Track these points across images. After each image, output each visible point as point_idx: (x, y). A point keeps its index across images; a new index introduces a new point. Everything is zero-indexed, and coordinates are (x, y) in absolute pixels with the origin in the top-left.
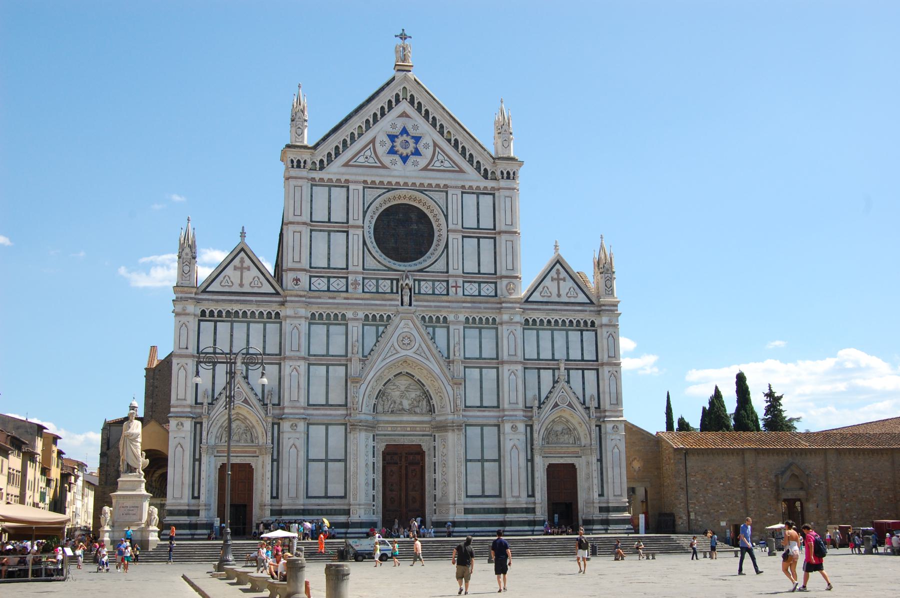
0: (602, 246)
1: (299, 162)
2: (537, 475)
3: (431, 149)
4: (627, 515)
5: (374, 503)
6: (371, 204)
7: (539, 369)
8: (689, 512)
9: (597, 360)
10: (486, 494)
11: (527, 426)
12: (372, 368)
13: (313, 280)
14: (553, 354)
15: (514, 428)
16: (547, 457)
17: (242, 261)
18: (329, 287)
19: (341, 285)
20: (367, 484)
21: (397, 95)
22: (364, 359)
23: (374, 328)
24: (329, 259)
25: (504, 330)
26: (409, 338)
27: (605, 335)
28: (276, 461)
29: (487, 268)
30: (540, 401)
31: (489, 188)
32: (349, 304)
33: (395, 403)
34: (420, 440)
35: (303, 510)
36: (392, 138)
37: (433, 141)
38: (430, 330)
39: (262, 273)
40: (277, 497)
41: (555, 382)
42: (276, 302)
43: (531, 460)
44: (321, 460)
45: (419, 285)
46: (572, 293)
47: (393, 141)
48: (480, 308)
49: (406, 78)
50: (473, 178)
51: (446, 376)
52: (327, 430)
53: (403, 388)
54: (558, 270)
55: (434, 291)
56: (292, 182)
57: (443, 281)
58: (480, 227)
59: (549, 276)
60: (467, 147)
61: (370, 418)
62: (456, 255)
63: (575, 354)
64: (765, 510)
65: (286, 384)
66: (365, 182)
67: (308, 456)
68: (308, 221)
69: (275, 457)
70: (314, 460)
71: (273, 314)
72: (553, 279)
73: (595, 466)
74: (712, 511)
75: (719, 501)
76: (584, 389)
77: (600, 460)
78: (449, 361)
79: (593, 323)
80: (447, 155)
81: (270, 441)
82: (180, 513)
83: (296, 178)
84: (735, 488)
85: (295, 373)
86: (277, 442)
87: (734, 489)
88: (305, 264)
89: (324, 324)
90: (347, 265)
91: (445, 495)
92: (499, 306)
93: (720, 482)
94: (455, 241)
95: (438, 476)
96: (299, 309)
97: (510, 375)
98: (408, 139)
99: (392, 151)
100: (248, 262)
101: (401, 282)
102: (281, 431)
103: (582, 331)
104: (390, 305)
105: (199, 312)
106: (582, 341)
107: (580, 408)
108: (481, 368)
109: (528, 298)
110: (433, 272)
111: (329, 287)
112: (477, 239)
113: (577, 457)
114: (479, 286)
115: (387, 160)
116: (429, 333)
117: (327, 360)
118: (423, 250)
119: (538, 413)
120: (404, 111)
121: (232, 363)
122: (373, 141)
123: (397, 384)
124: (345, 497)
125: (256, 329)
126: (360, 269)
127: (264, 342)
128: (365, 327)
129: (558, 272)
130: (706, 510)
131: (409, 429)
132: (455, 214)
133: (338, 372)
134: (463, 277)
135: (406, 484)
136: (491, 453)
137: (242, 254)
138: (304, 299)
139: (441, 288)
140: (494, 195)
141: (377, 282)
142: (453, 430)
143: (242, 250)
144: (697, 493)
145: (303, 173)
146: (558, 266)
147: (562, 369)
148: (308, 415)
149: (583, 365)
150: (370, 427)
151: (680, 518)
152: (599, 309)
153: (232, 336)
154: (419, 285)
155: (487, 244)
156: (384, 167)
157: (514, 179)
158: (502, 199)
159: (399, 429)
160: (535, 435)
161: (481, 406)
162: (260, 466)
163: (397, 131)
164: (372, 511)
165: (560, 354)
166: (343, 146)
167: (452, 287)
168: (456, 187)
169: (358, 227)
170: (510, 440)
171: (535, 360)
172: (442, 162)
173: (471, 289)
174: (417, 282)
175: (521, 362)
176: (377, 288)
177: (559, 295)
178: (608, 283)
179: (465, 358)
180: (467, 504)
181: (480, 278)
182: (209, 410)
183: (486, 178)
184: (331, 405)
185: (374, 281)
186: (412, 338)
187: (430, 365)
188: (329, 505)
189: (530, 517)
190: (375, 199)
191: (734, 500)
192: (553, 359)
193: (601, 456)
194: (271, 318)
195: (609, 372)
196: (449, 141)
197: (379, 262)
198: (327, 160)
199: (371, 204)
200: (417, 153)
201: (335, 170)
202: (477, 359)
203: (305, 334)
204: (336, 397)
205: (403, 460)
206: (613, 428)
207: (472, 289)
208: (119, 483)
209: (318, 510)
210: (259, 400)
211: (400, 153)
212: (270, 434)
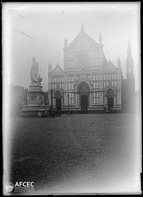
17: (58, 68)
28: (63, 99)
38: (87, 76)
41: (109, 84)
133: (73, 84)
143: (58, 65)
146: (110, 63)
150: (78, 93)
187: (87, 82)
212: (62, 95)
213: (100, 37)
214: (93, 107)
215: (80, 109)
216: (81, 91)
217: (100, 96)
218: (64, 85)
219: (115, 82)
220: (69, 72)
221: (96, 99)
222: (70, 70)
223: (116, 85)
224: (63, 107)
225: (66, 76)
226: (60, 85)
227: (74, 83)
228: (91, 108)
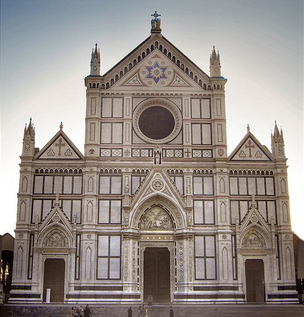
0: (276, 126)
2: (239, 266)
3: (172, 74)
4: (295, 292)
6: (137, 106)
7: (239, 201)
9: (275, 195)
11: (232, 236)
13: (102, 150)
14: (248, 192)
15: (224, 237)
17: (60, 141)
18: (111, 155)
19: (119, 153)
20: (134, 271)
21: (152, 46)
22: (132, 197)
24: (112, 138)
25: (217, 178)
27: (280, 179)
28: (78, 257)
29: (207, 141)
30: (240, 220)
32: (123, 164)
35: (94, 287)
36: (149, 69)
39: (72, 148)
40: (79, 279)
41: (249, 209)
42: (80, 163)
44: (106, 257)
45: (166, 152)
47: (150, 71)
48: (203, 164)
49: (157, 36)
51: (182, 206)
52: (109, 238)
53: (156, 214)
55: (174, 155)
56: (90, 96)
57: (180, 149)
60: (193, 73)
61: (136, 231)
63: (261, 192)
65: (85, 211)
66: (133, 94)
69: (78, 255)
70: (101, 257)
73: (275, 261)
76: (267, 213)
77: (278, 257)
79: (271, 172)
82: (20, 288)
83: (93, 93)
85: (90, 204)
86: (79, 245)
88: (97, 141)
90: (123, 142)
91: (182, 278)
92: (214, 163)
95: (178, 267)
96: (93, 168)
97: (221, 204)
98: (159, 69)
99: (149, 76)
100: (64, 141)
101: (154, 150)
102: (82, 239)
103: (265, 177)
104: (148, 164)
107: (266, 225)
108: (204, 200)
109: (231, 159)
111: (111, 155)
113: (263, 255)
114: (202, 152)
115: (146, 81)
116: (171, 180)
117: (110, 197)
120: (156, 55)
121: (52, 200)
122: (138, 71)
123: (153, 211)
124: (120, 279)
125: (68, 179)
127: (73, 187)
129: (250, 143)
131: (160, 238)
132: (187, 111)
136: (210, 253)
137: (61, 137)
139: (179, 153)
140: (210, 99)
141: (140, 151)
142: (187, 238)
143: (61, 135)
146: (249, 139)
147: (254, 200)
148: (98, 229)
149: (266, 198)
150: (136, 237)
152: (275, 164)
153: (53, 183)
154: (166, 152)
155: (206, 128)
156: (144, 85)
158: (215, 101)
159: (154, 238)
160: (238, 241)
162: (69, 259)
163: (153, 65)
165: (252, 192)
168: (187, 95)
169: (129, 119)
171: (237, 195)
172: (179, 81)
173: (197, 154)
174: (164, 150)
176: (140, 155)
177: (250, 156)
178: (281, 148)
180: (196, 284)
182: (38, 227)
185: (139, 151)
186: (161, 183)
190: (139, 104)
192: (248, 195)
194: (77, 173)
196: (183, 69)
197: (142, 139)
199: (137, 106)
200: (164, 77)
201: (116, 88)
204: (116, 219)
206: (286, 236)
207: (197, 154)
209: (103, 287)
210: (69, 221)
212: (75, 241)
214: (197, 292)
215: (141, 299)
216: (145, 232)
220: (106, 159)
221: (205, 260)
222: (107, 153)
224: (76, 288)
225: (92, 172)
226: (67, 204)
227: (121, 200)
228: (188, 296)
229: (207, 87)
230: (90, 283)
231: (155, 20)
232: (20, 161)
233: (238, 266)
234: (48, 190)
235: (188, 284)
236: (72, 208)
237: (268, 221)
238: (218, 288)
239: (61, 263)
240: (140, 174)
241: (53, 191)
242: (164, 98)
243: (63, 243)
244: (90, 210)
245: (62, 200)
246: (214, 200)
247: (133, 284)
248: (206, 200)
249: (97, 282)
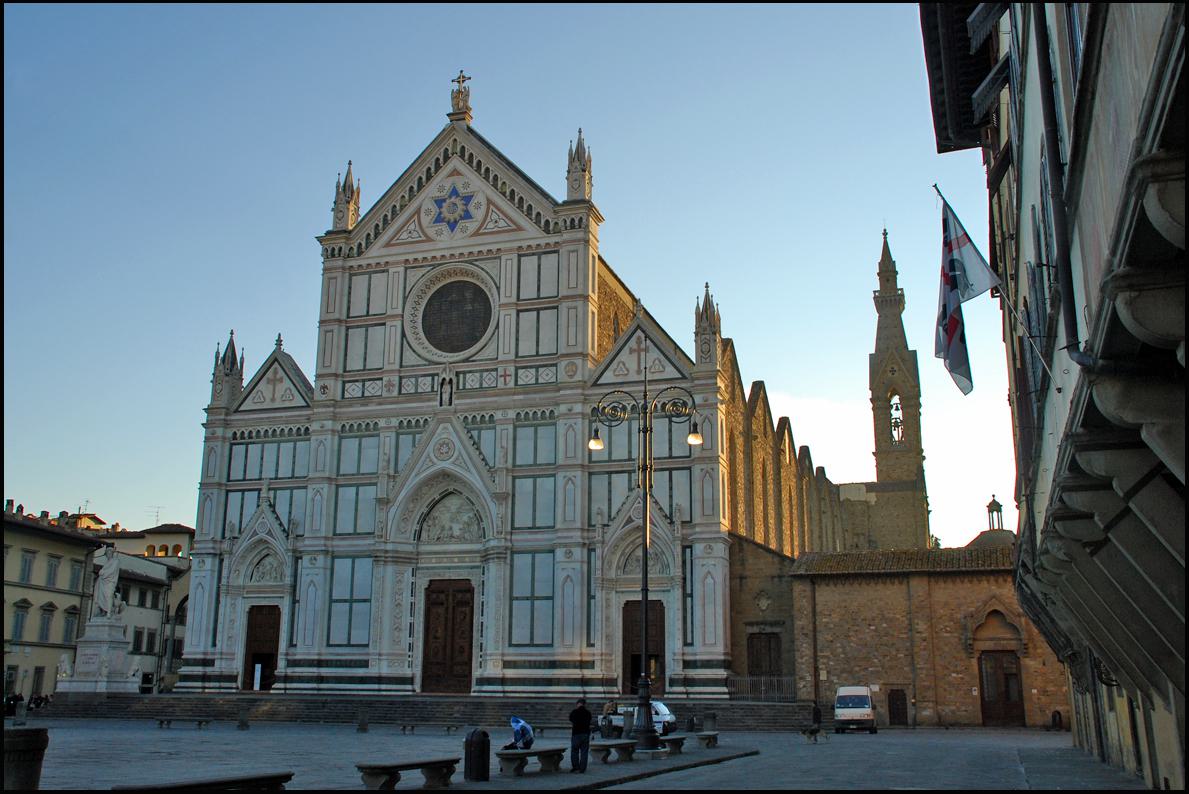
1: (333, 249)
3: (483, 208)
4: (722, 673)
5: (410, 653)
8: (816, 670)
10: (535, 643)
12: (403, 486)
13: (347, 385)
15: (569, 554)
16: (623, 592)
17: (276, 372)
20: (398, 628)
23: (411, 437)
24: (365, 359)
25: (561, 428)
26: (447, 445)
28: (294, 602)
30: (610, 516)
31: (552, 244)
33: (443, 528)
34: (469, 574)
36: (439, 202)
37: (488, 200)
41: (631, 489)
43: (590, 597)
44: (345, 601)
45: (464, 378)
46: (658, 367)
47: (440, 207)
48: (535, 399)
49: (454, 128)
50: (532, 235)
52: (353, 563)
53: (453, 509)
54: (639, 338)
55: (481, 384)
57: (493, 370)
58: (541, 296)
59: (626, 348)
61: (410, 548)
62: (507, 335)
64: (948, 668)
67: (331, 596)
68: (344, 317)
69: (297, 598)
71: (303, 430)
72: (631, 351)
74: (857, 669)
75: (869, 653)
76: (671, 497)
78: (492, 471)
80: (502, 212)
81: (288, 580)
84: (895, 634)
87: (893, 635)
89: (356, 437)
92: (557, 394)
93: (870, 625)
94: (503, 317)
95: (484, 619)
96: (325, 422)
97: (567, 483)
99: (439, 219)
100: (281, 373)
104: (429, 407)
105: (230, 434)
106: (670, 431)
108: (535, 477)
109: (598, 379)
110: (481, 360)
112: (535, 313)
113: (664, 591)
114: (537, 371)
115: (431, 232)
116: (471, 437)
117: (360, 480)
118: (478, 334)
119: (604, 533)
120: (455, 170)
121: (259, 490)
122: (418, 212)
124: (367, 646)
125: (287, 447)
126: (397, 366)
127: (294, 463)
128: (401, 436)
130: (846, 666)
131: (456, 560)
134: (515, 361)
135: (453, 630)
137: (276, 365)
138: (332, 409)
139: (489, 379)
142: (493, 559)
143: (276, 360)
144: (832, 641)
145: (339, 263)
146: (639, 332)
148: (332, 546)
150: (409, 560)
151: (801, 678)
153: (262, 458)
154: (464, 378)
156: (429, 239)
157: (580, 227)
159: (445, 560)
161: (534, 527)
163: (445, 194)
164: (407, 664)
166: (384, 224)
167: (501, 376)
168: (510, 250)
170: (563, 569)
172: (496, 222)
175: (582, 466)
176: (417, 388)
179: (514, 465)
180: (509, 655)
181: (537, 360)
183: (548, 232)
184: (359, 534)
185: (413, 380)
188: (349, 654)
189: (588, 673)
191: (894, 653)
193: (692, 590)
195: (702, 470)
196: (504, 194)
197: (419, 356)
198: (367, 244)
200: (467, 216)
201: (376, 253)
202: (531, 465)
203: (332, 451)
205: (451, 598)
206: (705, 547)
207: (527, 377)
208: (87, 628)
209: (337, 661)
211: (446, 220)
212: (288, 572)
213: (579, 162)
215: (418, 687)
217: (558, 591)
218: (310, 496)
219: (680, 477)
221: (533, 606)
223: (681, 499)
226: (283, 497)
227: (375, 484)
229: (551, 228)
230: (309, 654)
231: (459, 92)
232: (204, 417)
233: (598, 616)
234: (253, 473)
235: (491, 655)
236: (291, 505)
237: (671, 514)
238: (553, 665)
239: (274, 611)
240: (410, 427)
241: (261, 472)
242: (466, 262)
243: (279, 577)
244: (317, 509)
245: (275, 489)
246: (554, 475)
247: (389, 655)
248: (539, 476)
249: (325, 650)
